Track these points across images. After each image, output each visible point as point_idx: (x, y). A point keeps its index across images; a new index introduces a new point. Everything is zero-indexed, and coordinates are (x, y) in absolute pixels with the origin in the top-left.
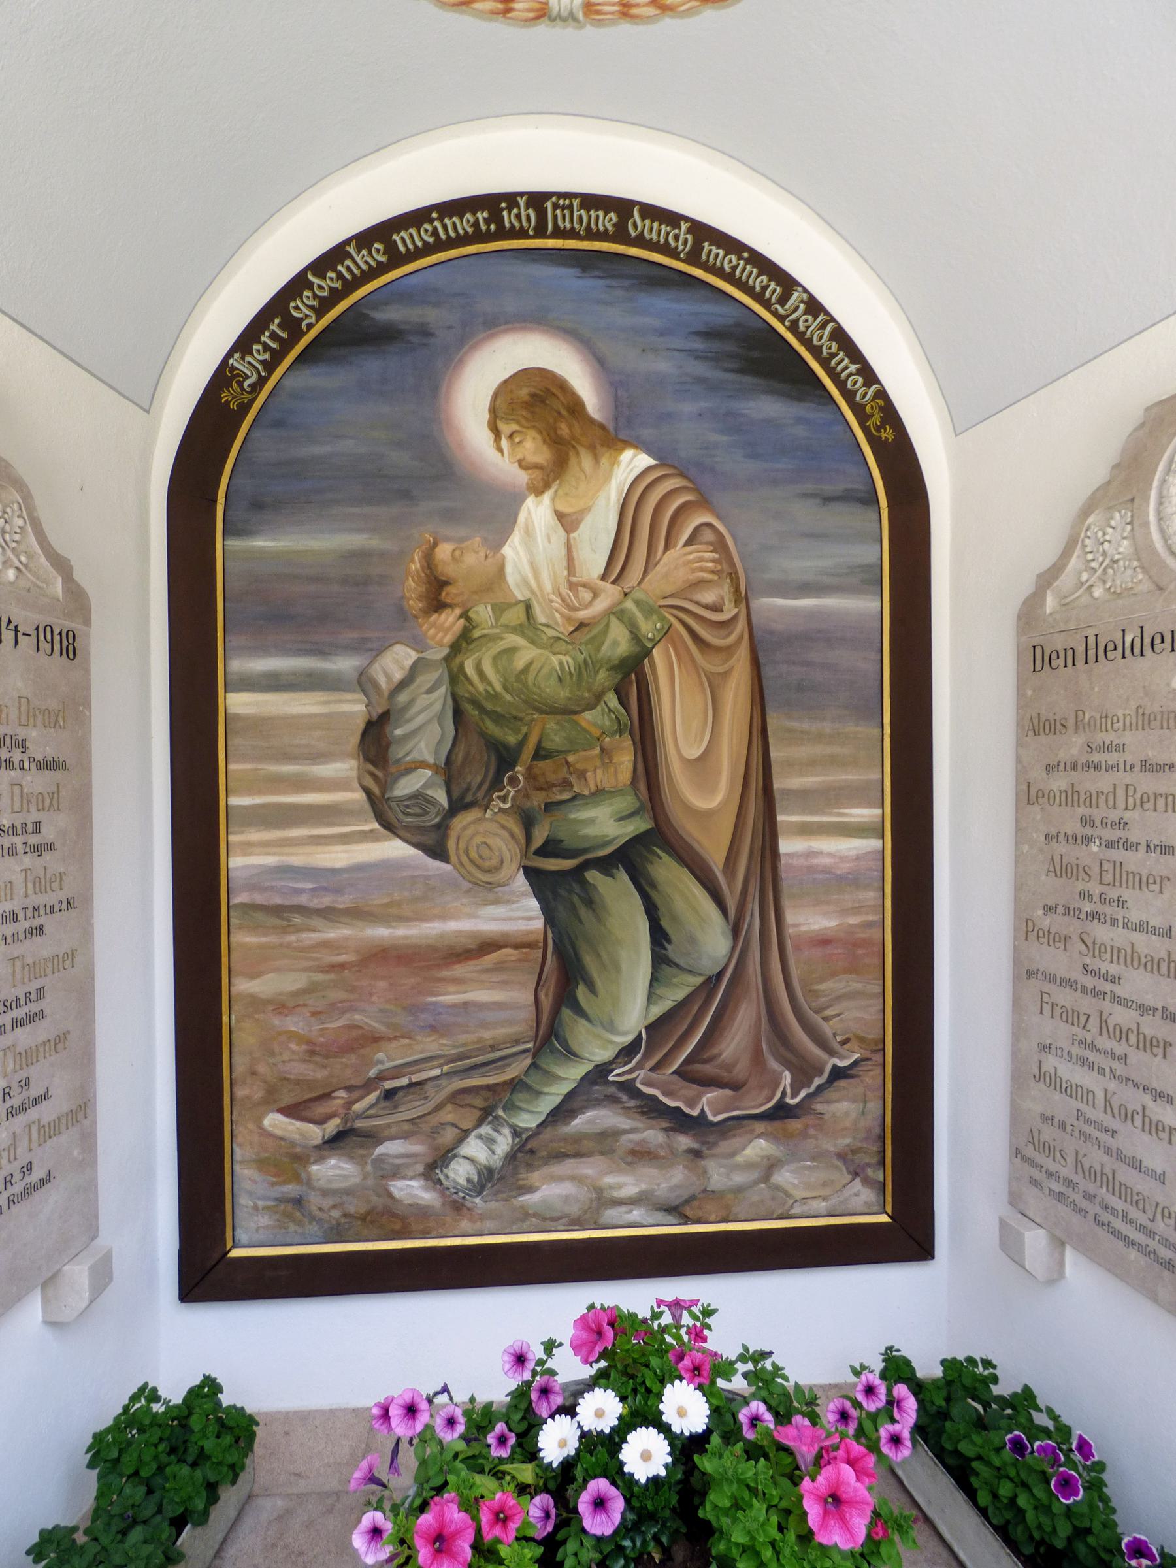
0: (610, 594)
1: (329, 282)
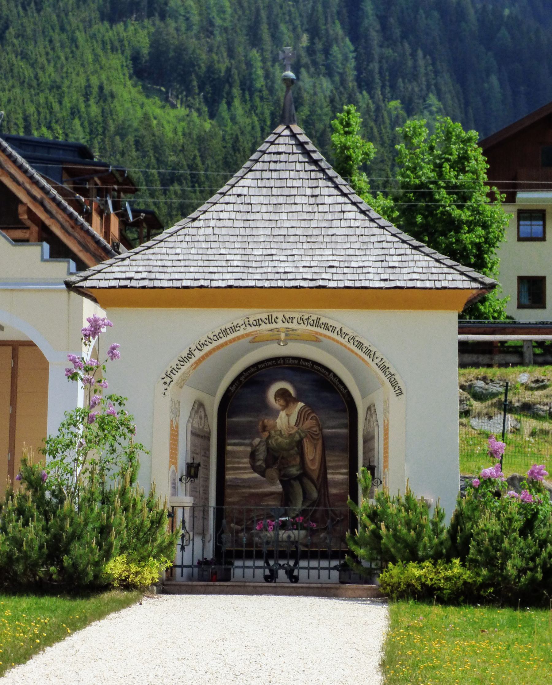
0: (296, 429)
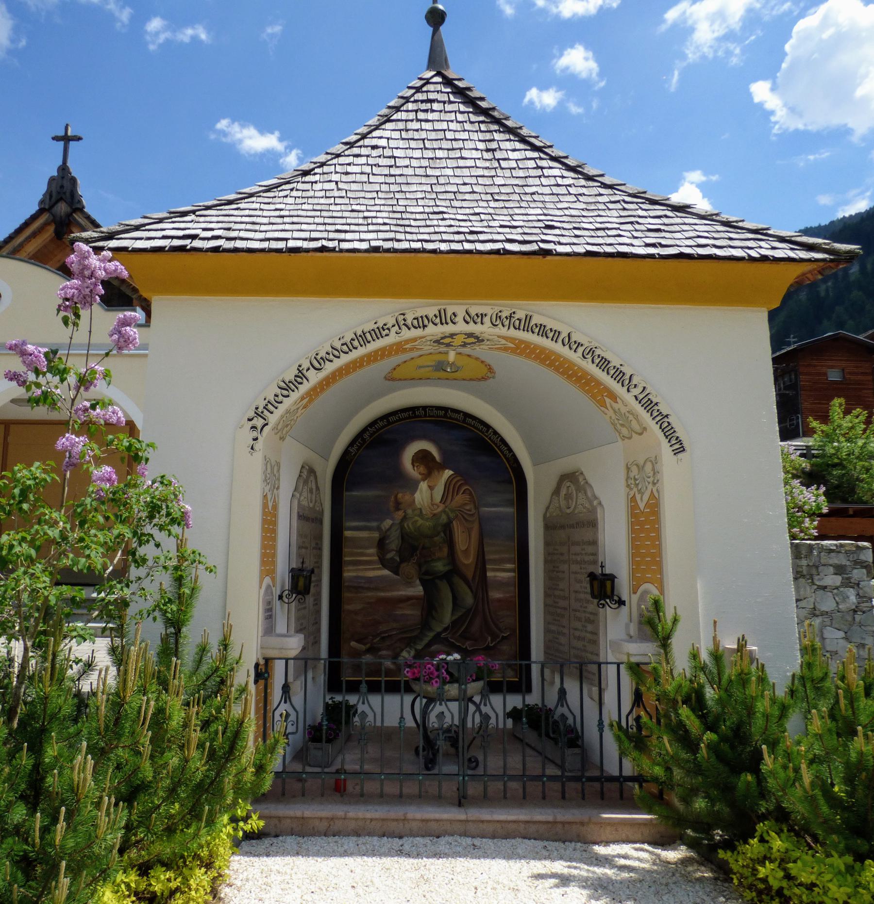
0: (442, 507)
1: (373, 429)
